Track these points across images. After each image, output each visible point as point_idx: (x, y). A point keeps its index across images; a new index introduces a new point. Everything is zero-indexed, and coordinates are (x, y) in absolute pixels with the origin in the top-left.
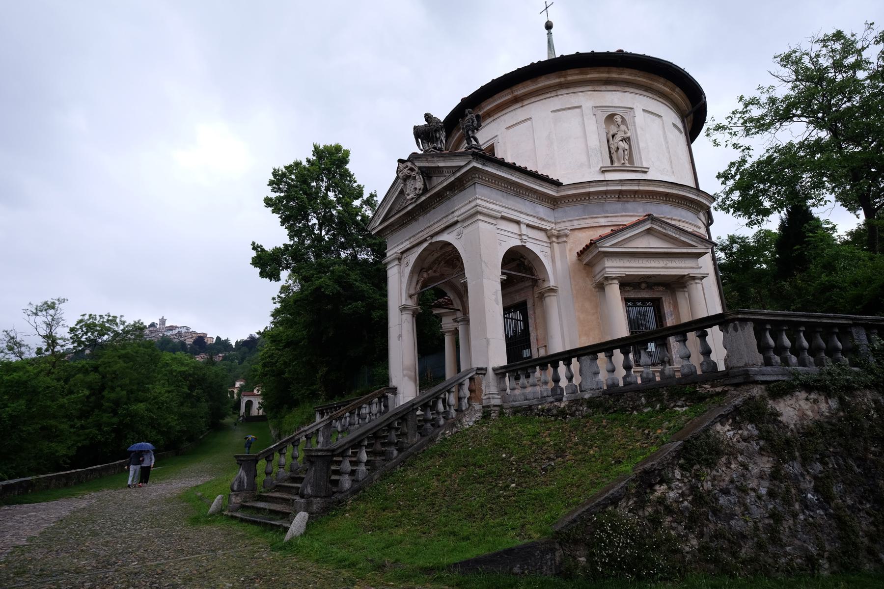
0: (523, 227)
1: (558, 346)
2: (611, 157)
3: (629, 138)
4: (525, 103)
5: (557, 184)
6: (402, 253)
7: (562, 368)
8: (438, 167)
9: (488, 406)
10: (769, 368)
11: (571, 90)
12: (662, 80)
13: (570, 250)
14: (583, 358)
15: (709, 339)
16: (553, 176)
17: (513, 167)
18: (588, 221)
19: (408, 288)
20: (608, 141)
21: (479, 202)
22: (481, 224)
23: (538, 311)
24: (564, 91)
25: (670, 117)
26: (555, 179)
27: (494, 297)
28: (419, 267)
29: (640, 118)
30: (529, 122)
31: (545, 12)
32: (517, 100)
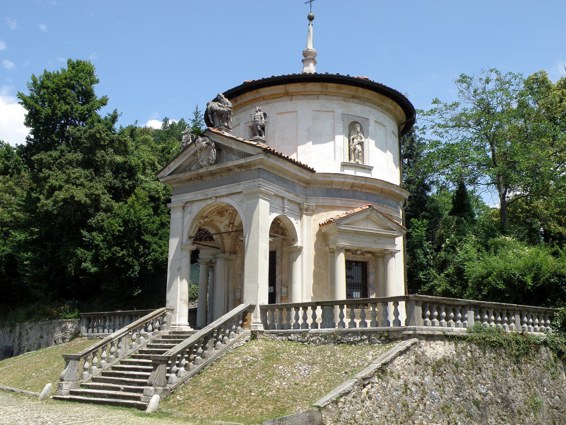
2: (349, 155)
3: (363, 143)
4: (294, 98)
5: (312, 171)
6: (186, 202)
7: (310, 311)
9: (256, 331)
10: (426, 327)
11: (328, 97)
12: (390, 100)
13: (314, 220)
14: (325, 307)
15: (399, 307)
16: (310, 166)
17: (287, 159)
18: (329, 201)
19: (189, 232)
21: (261, 183)
22: (261, 200)
24: (325, 96)
25: (392, 127)
28: (201, 216)
29: (372, 127)
30: (295, 114)
31: (309, 4)
32: (287, 94)
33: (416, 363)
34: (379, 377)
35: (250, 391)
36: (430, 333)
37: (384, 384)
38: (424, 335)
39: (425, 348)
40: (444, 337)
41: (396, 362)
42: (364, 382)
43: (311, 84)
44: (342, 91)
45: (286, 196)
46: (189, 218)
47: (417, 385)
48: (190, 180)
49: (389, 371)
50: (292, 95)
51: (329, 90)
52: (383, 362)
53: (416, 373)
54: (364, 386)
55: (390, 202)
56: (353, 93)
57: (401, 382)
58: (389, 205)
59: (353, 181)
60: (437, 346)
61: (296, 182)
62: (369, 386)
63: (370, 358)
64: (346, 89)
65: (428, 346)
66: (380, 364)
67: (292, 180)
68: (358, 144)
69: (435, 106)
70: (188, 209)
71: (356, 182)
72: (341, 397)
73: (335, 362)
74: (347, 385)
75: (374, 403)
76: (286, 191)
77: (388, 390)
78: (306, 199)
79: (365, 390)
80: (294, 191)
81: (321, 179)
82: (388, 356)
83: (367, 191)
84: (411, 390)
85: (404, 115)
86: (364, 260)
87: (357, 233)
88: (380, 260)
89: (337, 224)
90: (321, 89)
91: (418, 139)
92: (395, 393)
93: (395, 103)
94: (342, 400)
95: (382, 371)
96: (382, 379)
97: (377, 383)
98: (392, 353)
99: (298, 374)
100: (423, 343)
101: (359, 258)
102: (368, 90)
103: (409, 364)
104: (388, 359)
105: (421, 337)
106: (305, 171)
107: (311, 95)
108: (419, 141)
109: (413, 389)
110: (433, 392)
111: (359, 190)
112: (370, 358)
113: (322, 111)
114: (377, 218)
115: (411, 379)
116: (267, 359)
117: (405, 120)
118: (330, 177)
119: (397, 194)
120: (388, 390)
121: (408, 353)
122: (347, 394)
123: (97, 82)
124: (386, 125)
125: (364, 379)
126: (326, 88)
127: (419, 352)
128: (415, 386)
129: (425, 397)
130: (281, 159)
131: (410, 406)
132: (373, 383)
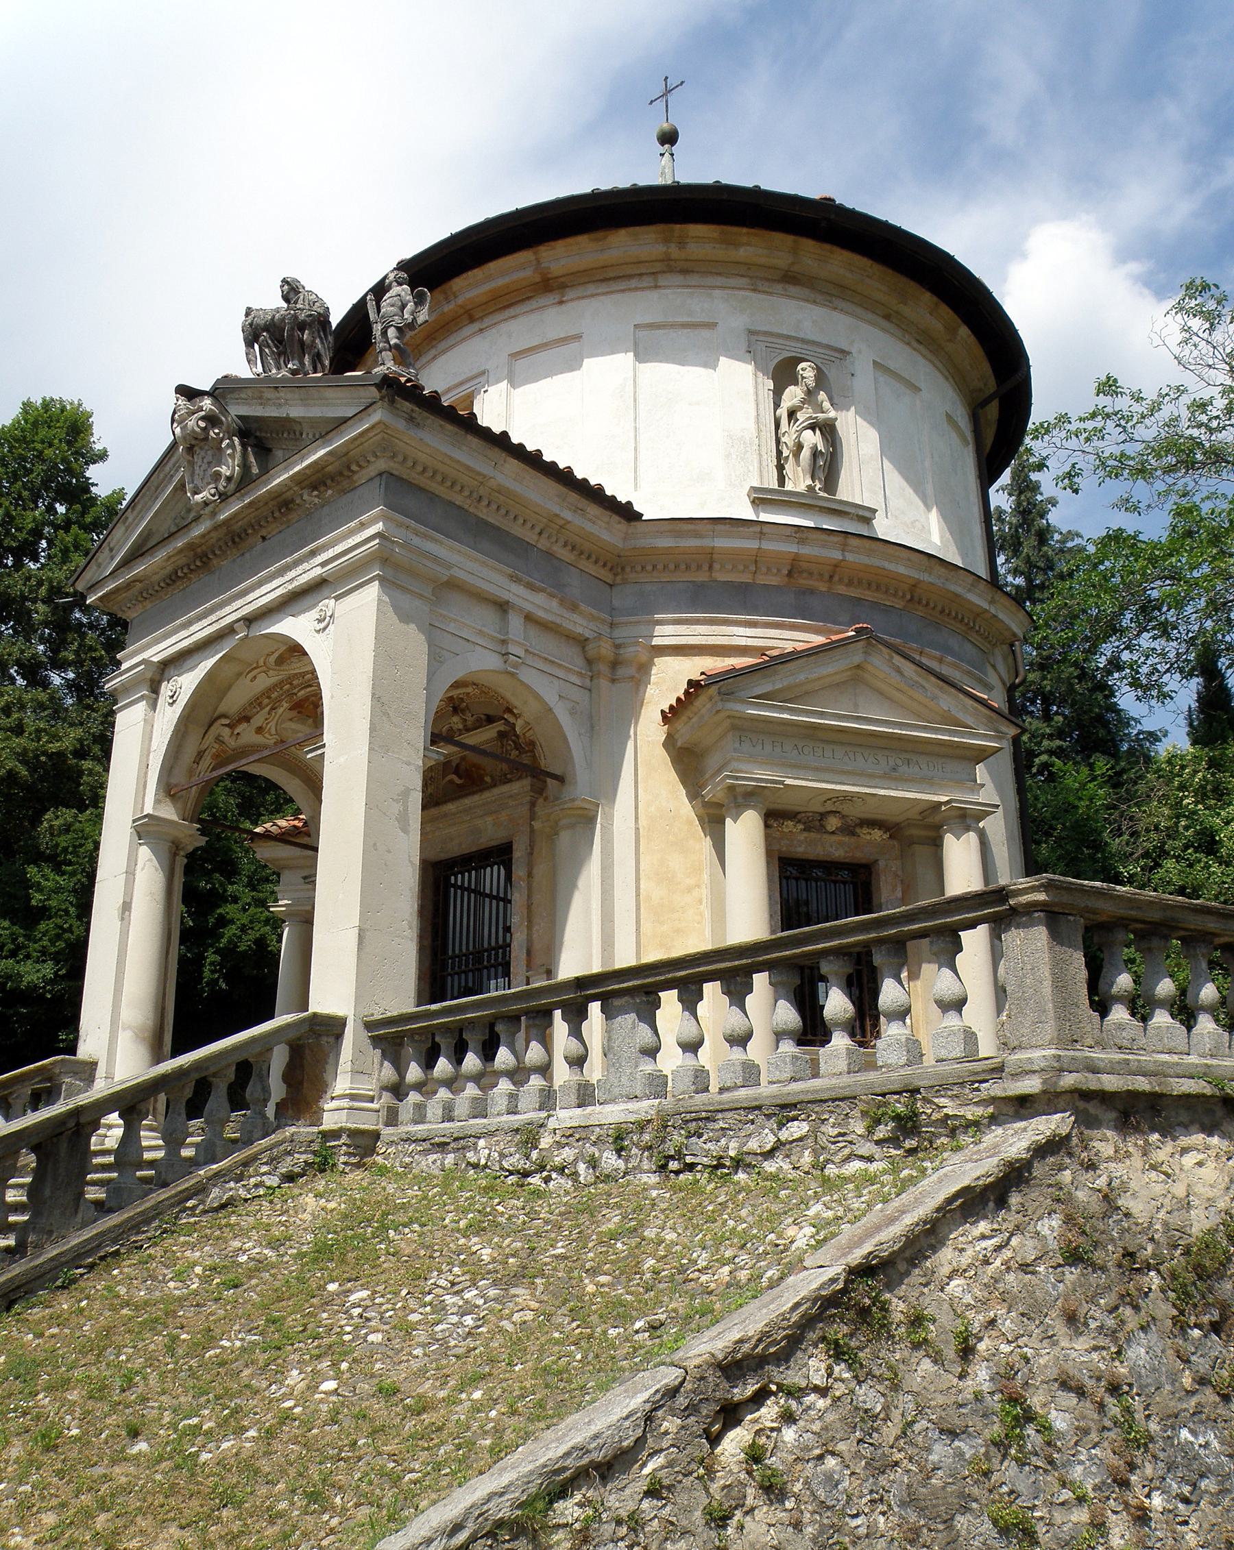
0: (516, 622)
1: (572, 963)
2: (780, 468)
4: (570, 294)
5: (627, 513)
8: (288, 420)
11: (694, 279)
12: (927, 297)
16: (618, 489)
20: (777, 425)
23: (540, 870)
24: (678, 279)
26: (622, 499)
27: (396, 808)
29: (864, 379)
31: (661, 104)
32: (549, 286)
33: (1074, 1257)
34: (838, 1352)
35: (134, 1434)
36: (1142, 1084)
37: (869, 1396)
38: (1103, 1097)
39: (1118, 1170)
40: (1220, 1112)
41: (946, 1258)
42: (746, 1377)
43: (623, 232)
44: (743, 253)
45: (512, 599)
46: (167, 717)
47: (1081, 1392)
48: (173, 579)
49: (899, 1309)
50: (563, 287)
51: (695, 250)
52: (856, 1257)
53: (1071, 1318)
54: (731, 1415)
55: (954, 642)
56: (782, 260)
57: (981, 1375)
58: (949, 650)
59: (792, 548)
60: (1189, 1160)
61: (565, 554)
62: (768, 1412)
63: (802, 1236)
64: (754, 246)
65: (1137, 1161)
66: (837, 1269)
67: (543, 544)
68: (812, 427)
69: (1103, 400)
70: (166, 689)
71: (805, 550)
72: (562, 1492)
73: (628, 1269)
74: (607, 1416)
75: (797, 1526)
76: (515, 579)
77: (891, 1431)
78: (612, 625)
79: (734, 1442)
80: (556, 589)
81: (665, 542)
82: (892, 1220)
83: (854, 593)
84: (1045, 1428)
85: (986, 368)
86: (860, 856)
87: (812, 733)
88: (921, 851)
89: (726, 695)
90: (659, 250)
91: (1057, 537)
92: (940, 1452)
93: (945, 310)
94: (569, 1510)
95: (857, 1307)
96: (852, 1362)
97: (823, 1392)
98: (918, 1202)
99: (421, 1335)
100: (1105, 1142)
101: (834, 848)
102: (837, 250)
103: (1025, 1268)
104: (890, 1235)
105: (1093, 1108)
106: (594, 510)
107: (630, 277)
108: (1063, 542)
109: (1060, 1422)
110: (1185, 1434)
111: (823, 587)
112: (802, 1236)
113: (673, 326)
114: (895, 679)
115: (1045, 1360)
116: (322, 1252)
117: (992, 385)
118: (697, 535)
119: (980, 614)
120: (891, 1431)
121: (1014, 1199)
122: (610, 1466)
123: (102, 456)
124: (922, 385)
125: (732, 1367)
126: (682, 244)
127: (1081, 1195)
128: (1071, 1400)
129: (1132, 1467)
130: (474, 441)
131: (1041, 1529)
132: (795, 1393)
